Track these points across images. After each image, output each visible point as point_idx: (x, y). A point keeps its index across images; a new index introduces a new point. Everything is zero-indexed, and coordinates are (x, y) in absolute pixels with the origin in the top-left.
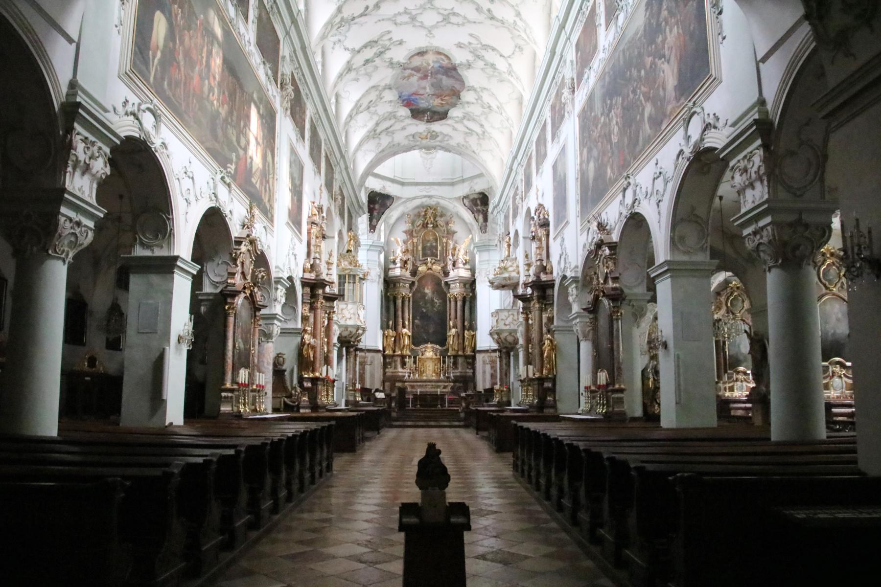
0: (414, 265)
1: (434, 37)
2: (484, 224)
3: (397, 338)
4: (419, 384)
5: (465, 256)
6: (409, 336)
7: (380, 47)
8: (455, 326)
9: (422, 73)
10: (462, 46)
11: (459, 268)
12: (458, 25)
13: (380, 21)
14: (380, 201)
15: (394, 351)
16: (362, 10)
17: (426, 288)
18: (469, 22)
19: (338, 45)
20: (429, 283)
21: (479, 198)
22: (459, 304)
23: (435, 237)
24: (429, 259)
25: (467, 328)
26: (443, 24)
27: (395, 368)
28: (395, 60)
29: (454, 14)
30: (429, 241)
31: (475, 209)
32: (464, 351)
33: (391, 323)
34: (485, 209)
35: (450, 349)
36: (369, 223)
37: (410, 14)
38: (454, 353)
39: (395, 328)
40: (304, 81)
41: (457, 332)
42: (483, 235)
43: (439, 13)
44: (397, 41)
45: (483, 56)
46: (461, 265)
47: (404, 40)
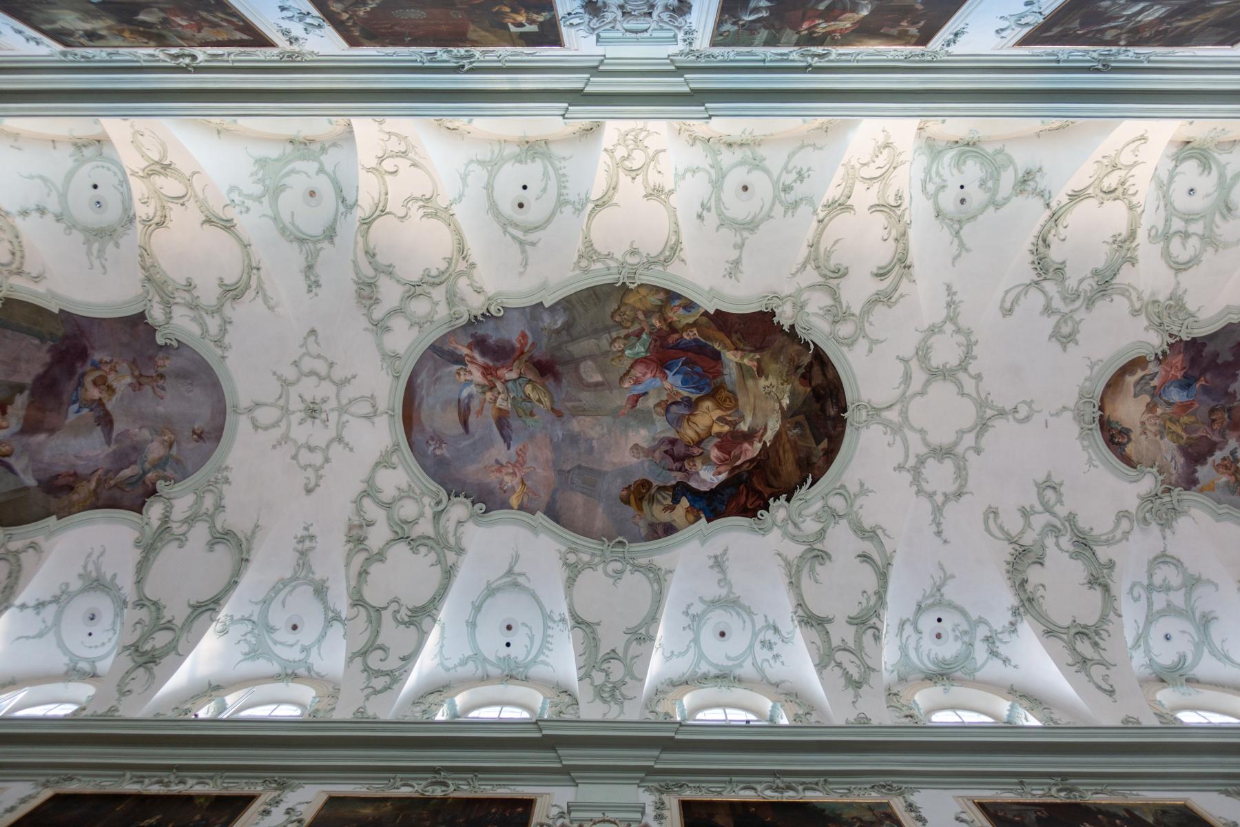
1: (1029, 404)
7: (1050, 541)
9: (1223, 436)
10: (1066, 330)
12: (969, 346)
13: (939, 533)
16: (867, 568)
18: (952, 319)
19: (998, 644)
26: (969, 385)
28: (1132, 504)
29: (923, 353)
37: (921, 461)
40: (816, 780)
43: (922, 393)
44: (1040, 496)
45: (1095, 273)
47: (1041, 477)
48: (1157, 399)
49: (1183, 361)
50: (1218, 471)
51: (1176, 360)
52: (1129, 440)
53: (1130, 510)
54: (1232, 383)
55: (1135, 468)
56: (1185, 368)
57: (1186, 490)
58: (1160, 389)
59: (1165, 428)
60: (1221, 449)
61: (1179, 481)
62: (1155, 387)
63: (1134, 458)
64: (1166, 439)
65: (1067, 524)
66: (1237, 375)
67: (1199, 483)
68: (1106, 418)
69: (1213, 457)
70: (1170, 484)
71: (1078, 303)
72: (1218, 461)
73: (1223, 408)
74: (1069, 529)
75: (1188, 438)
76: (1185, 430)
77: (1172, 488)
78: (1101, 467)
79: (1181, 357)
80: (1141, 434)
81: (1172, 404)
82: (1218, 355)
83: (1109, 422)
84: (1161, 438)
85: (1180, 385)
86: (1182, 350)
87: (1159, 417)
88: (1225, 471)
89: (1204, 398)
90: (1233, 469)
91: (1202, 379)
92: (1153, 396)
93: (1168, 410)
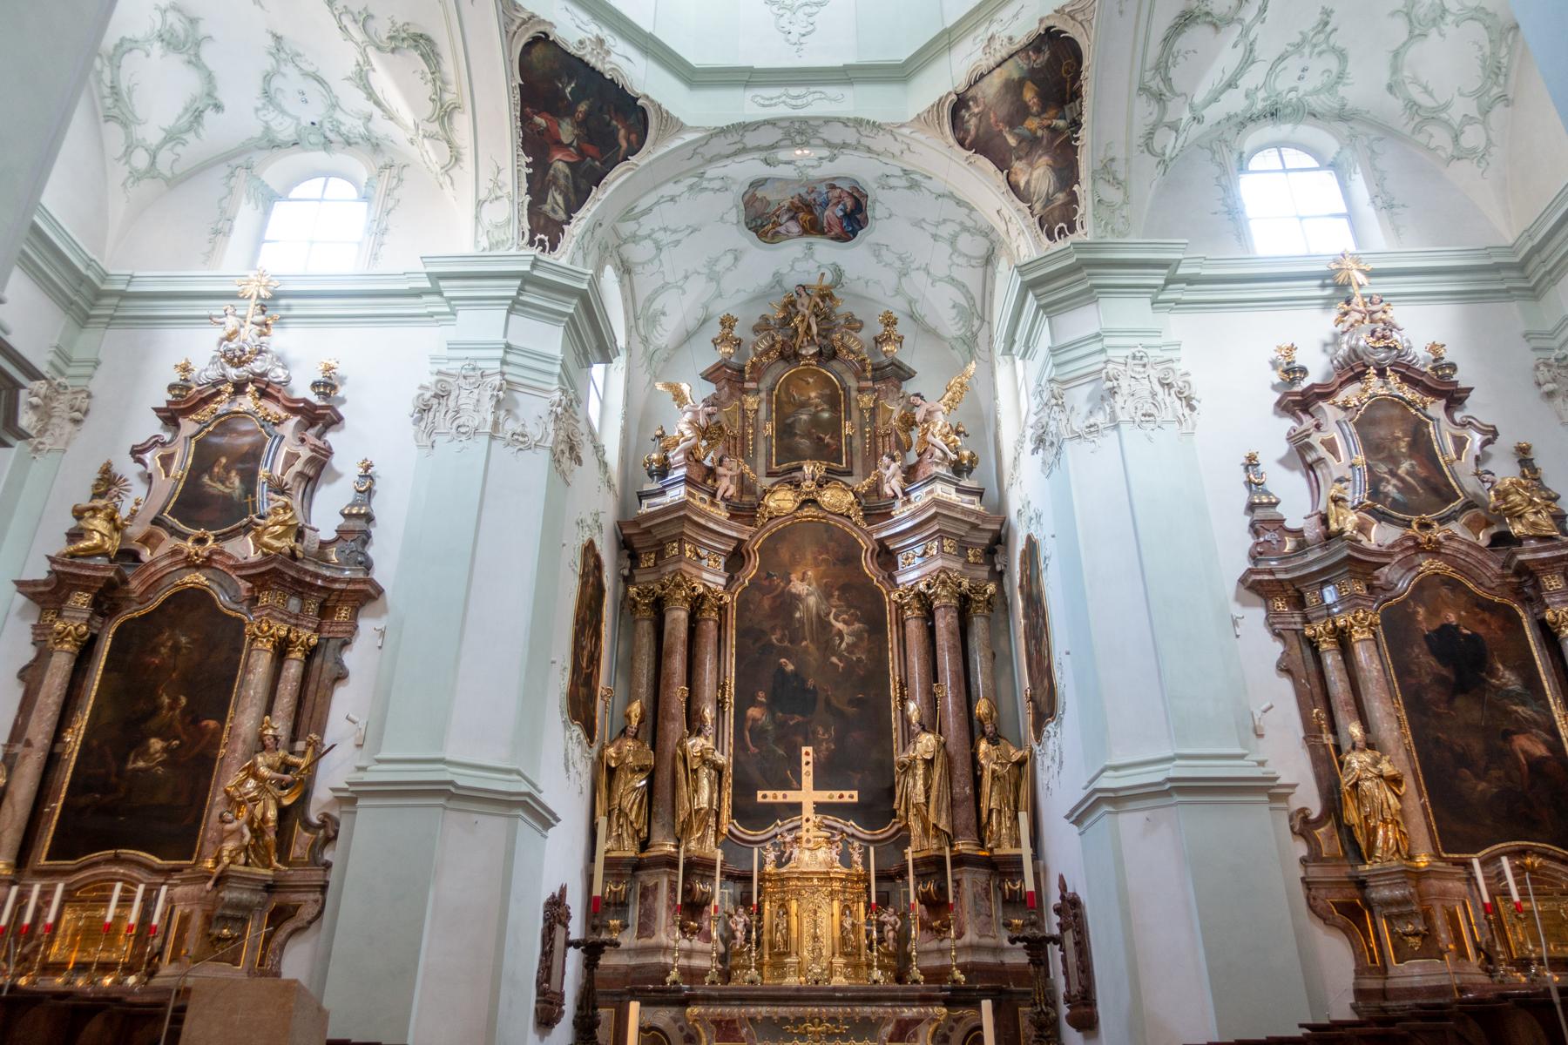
0: (744, 485)
2: (1061, 197)
3: (664, 777)
4: (763, 1011)
5: (953, 437)
6: (719, 770)
8: (932, 723)
11: (933, 479)
14: (583, 107)
15: (644, 845)
17: (793, 577)
20: (809, 557)
21: (1033, 75)
22: (945, 622)
23: (828, 391)
24: (808, 468)
25: (989, 728)
27: (645, 928)
30: (803, 405)
31: (1012, 141)
32: (981, 844)
33: (636, 708)
34: (1061, 123)
35: (916, 827)
36: (528, 198)
38: (931, 847)
39: (653, 728)
41: (943, 745)
42: (1061, 244)
46: (942, 470)
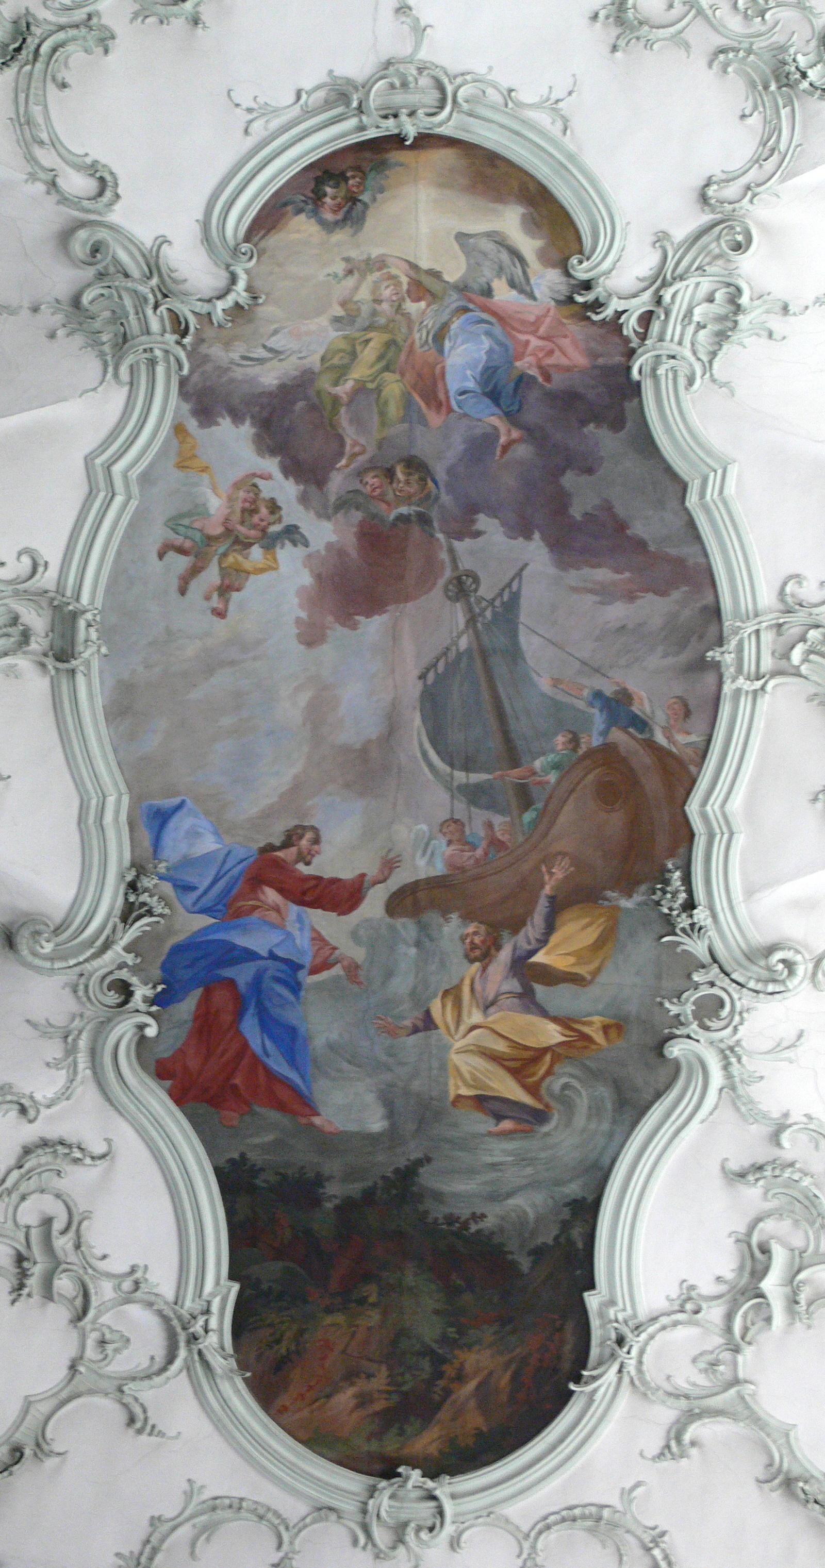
9: (342, 505)
48: (454, 300)
49: (568, 369)
50: (237, 486)
51: (570, 350)
52: (329, 227)
53: (117, 207)
54: (504, 524)
55: (247, 239)
56: (548, 378)
57: (183, 382)
58: (485, 309)
59: (367, 329)
60: (304, 499)
61: (208, 367)
62: (488, 292)
63: (274, 240)
64: (333, 334)
65: (79, 15)
66: (528, 537)
67: (202, 425)
68: (396, 156)
69: (278, 475)
70: (200, 340)
71: (735, 24)
72: (267, 490)
73: (427, 499)
74: (63, 20)
75: (336, 400)
76: (360, 389)
77: (187, 340)
78: (250, 142)
79: (580, 360)
80: (347, 260)
81: (441, 351)
82: (590, 471)
83: (381, 166)
84: (337, 320)
85: (496, 369)
86: (601, 361)
87: (399, 309)
88: (238, 506)
89: (457, 446)
90: (242, 529)
91: (515, 434)
92: (462, 288)
93: (419, 337)
